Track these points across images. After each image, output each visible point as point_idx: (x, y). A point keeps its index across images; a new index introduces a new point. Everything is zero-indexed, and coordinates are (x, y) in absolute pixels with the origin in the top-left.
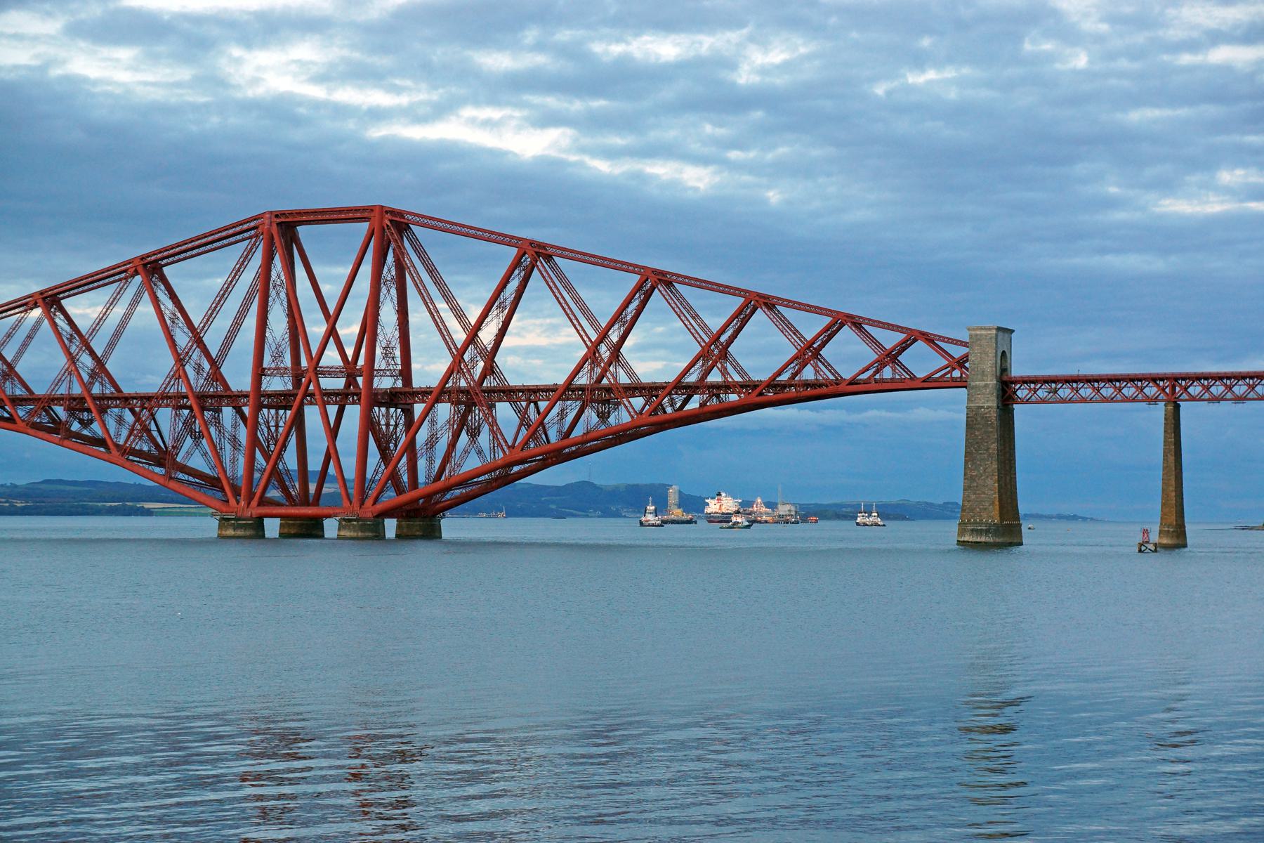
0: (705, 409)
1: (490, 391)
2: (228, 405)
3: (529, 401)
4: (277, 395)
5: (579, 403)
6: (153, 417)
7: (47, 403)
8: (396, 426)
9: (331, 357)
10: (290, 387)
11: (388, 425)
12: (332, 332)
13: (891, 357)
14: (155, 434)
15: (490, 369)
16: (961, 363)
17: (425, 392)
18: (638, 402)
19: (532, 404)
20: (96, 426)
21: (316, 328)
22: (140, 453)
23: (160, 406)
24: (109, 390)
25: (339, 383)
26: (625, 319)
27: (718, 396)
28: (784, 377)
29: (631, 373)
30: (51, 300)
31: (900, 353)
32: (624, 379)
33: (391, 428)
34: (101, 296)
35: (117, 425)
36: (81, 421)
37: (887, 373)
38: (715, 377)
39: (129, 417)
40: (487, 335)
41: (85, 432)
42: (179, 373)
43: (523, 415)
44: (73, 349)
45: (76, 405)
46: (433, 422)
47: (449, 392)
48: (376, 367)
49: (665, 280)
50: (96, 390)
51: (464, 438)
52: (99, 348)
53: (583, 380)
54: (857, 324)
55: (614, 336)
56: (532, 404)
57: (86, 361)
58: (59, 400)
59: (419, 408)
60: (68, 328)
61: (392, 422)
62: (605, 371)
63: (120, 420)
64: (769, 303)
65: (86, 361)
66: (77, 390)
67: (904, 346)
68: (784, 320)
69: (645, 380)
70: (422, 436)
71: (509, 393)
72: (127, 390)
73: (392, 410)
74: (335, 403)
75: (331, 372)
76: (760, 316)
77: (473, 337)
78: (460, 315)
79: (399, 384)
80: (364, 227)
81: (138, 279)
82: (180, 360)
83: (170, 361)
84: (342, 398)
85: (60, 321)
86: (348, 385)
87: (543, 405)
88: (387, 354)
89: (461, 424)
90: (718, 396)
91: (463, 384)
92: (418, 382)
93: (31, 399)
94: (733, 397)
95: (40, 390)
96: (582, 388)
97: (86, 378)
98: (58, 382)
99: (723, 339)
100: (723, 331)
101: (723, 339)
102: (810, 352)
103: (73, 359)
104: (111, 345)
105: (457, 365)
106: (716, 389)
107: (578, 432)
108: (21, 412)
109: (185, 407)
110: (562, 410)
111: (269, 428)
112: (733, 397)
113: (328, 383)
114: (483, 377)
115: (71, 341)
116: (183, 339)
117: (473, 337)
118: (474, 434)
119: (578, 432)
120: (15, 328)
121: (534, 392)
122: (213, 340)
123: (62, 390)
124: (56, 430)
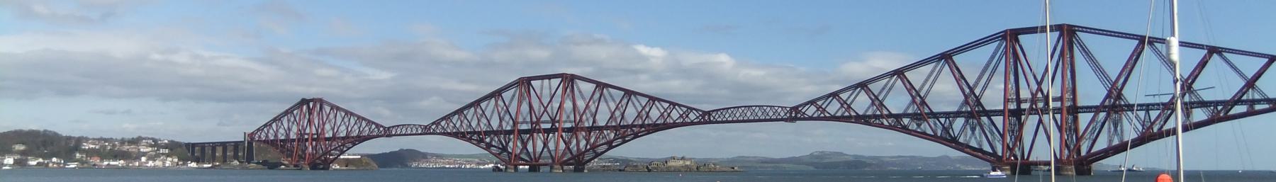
4: (1010, 111)
6: (951, 124)
7: (898, 117)
9: (1040, 95)
10: (1016, 107)
15: (1119, 96)
17: (1088, 109)
24: (927, 111)
30: (899, 73)
34: (927, 69)
38: (1250, 95)
41: (919, 130)
42: (966, 102)
45: (914, 117)
47: (1106, 107)
49: (1213, 50)
53: (1107, 103)
58: (905, 115)
59: (1023, 117)
69: (1207, 96)
75: (1041, 101)
83: (963, 98)
86: (1044, 106)
92: (1080, 103)
93: (890, 115)
95: (894, 112)
98: (908, 108)
103: (913, 98)
104: (928, 92)
105: (1108, 96)
106: (1253, 102)
120: (886, 85)
121: (1147, 107)
123: (910, 111)
124: (905, 130)
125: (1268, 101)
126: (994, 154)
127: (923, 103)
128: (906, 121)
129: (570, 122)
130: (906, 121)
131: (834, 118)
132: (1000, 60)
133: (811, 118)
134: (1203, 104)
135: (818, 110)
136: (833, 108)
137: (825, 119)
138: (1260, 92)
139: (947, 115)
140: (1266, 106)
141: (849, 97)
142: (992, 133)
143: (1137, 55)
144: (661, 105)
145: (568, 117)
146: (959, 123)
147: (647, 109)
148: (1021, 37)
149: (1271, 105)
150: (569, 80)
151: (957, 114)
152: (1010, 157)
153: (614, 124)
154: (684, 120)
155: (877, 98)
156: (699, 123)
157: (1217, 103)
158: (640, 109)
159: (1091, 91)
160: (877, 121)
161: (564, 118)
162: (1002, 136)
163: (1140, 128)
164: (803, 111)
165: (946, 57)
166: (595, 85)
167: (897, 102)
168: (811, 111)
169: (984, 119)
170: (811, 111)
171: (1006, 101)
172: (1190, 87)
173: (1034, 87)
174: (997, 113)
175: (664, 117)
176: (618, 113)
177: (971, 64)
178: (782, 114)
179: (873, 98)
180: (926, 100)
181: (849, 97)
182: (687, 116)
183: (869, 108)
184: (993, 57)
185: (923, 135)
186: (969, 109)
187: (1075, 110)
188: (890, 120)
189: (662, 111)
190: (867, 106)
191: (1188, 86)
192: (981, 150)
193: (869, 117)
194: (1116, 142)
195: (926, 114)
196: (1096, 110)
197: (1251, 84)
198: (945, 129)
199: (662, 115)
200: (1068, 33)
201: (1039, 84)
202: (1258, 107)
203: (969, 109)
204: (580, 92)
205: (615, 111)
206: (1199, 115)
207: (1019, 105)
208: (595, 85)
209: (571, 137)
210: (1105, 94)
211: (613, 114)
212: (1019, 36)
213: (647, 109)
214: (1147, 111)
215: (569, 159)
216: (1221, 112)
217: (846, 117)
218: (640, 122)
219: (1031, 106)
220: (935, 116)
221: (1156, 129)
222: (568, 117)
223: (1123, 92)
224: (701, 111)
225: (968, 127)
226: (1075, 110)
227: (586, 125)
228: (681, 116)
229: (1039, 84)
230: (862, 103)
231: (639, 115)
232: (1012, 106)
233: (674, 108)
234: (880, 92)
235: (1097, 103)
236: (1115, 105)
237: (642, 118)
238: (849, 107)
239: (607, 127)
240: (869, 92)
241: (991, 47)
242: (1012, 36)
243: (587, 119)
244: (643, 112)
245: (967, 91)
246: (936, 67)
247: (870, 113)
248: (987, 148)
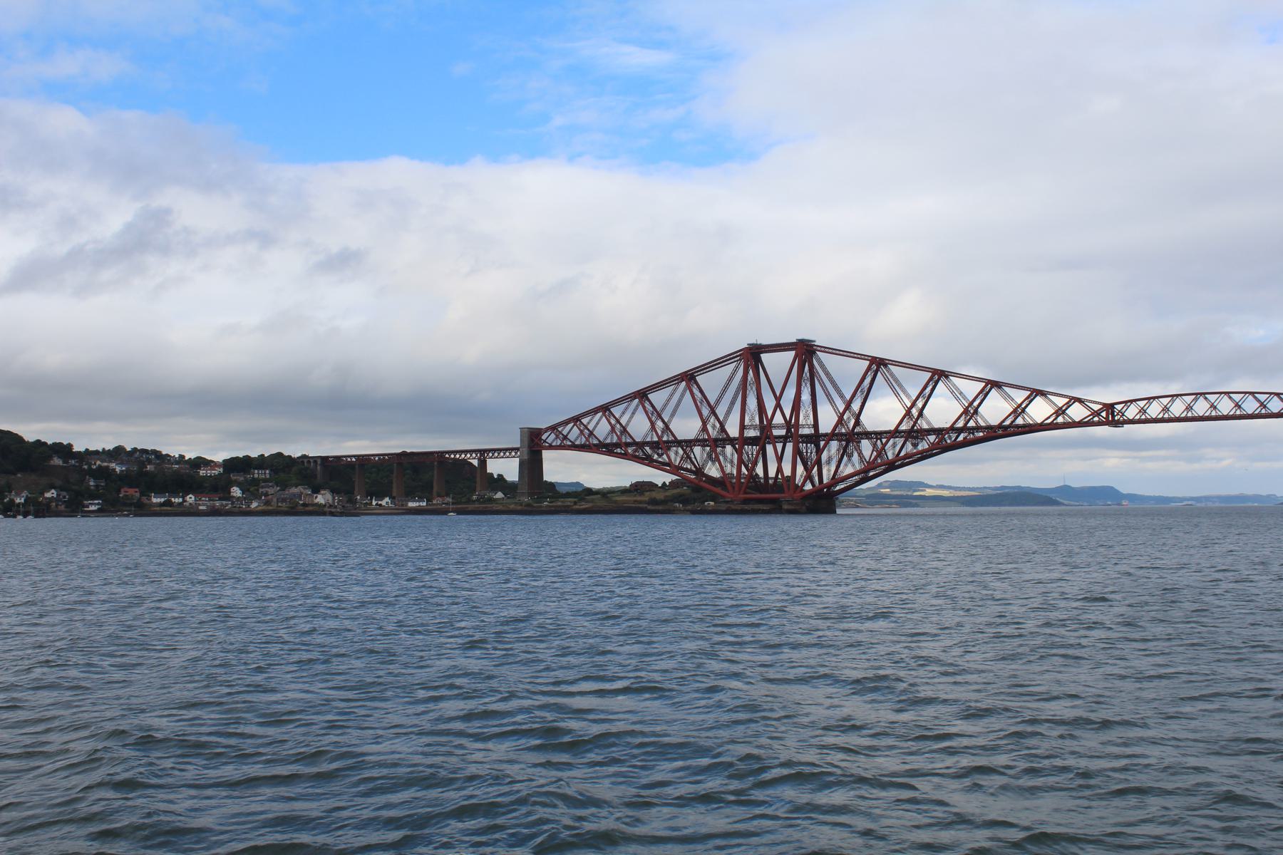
0: (966, 440)
1: (858, 434)
2: (728, 444)
3: (877, 439)
5: (903, 439)
7: (641, 445)
8: (811, 453)
9: (778, 419)
10: (758, 434)
11: (807, 452)
12: (778, 406)
14: (694, 459)
15: (857, 423)
16: (1097, 413)
17: (826, 435)
18: (932, 438)
19: (879, 441)
20: (665, 456)
21: (770, 404)
22: (686, 470)
23: (695, 446)
24: (671, 438)
25: (783, 432)
26: (926, 394)
27: (973, 434)
28: (1007, 423)
29: (928, 423)
31: (1066, 409)
32: (925, 426)
33: (809, 454)
35: (675, 455)
36: (658, 454)
37: (1060, 420)
38: (971, 424)
39: (681, 451)
40: (856, 406)
41: (660, 460)
42: (704, 429)
43: (874, 445)
44: (653, 419)
45: (654, 446)
46: (829, 451)
47: (837, 435)
48: (800, 423)
50: (665, 438)
51: (845, 458)
53: (904, 427)
55: (920, 404)
56: (879, 441)
57: (659, 424)
58: (647, 443)
59: (822, 443)
60: (651, 409)
61: (809, 451)
62: (915, 423)
63: (677, 453)
64: (996, 385)
65: (659, 424)
66: (656, 439)
67: (1068, 405)
68: (1006, 393)
69: (936, 426)
70: (824, 456)
71: (867, 435)
73: (809, 445)
74: (781, 442)
75: (778, 427)
77: (848, 406)
78: (842, 396)
81: (684, 383)
82: (704, 423)
84: (784, 439)
85: (647, 405)
86: (787, 432)
87: (884, 440)
88: (806, 416)
89: (844, 452)
90: (973, 434)
91: (843, 431)
93: (634, 443)
94: (981, 434)
96: (903, 431)
97: (660, 433)
98: (646, 435)
99: (976, 404)
100: (974, 400)
101: (976, 404)
102: (1019, 411)
103: (653, 424)
105: (840, 421)
107: (902, 454)
108: (630, 450)
109: (707, 446)
110: (894, 443)
111: (748, 456)
112: (981, 434)
113: (776, 432)
114: (854, 427)
115: (652, 414)
116: (706, 412)
117: (848, 406)
118: (850, 456)
119: (902, 454)
121: (879, 435)
122: (721, 412)
123: (648, 439)
125: (989, 428)
131: (574, 447)
135: (557, 437)
139: (688, 444)
141: (588, 423)
148: (764, 357)
155: (618, 421)
159: (827, 421)
160: (619, 450)
179: (613, 421)
185: (661, 466)
195: (667, 442)
197: (970, 411)
198: (687, 457)
220: (679, 443)
230: (602, 428)
238: (591, 433)
242: (752, 355)
246: (675, 390)
247: (608, 441)
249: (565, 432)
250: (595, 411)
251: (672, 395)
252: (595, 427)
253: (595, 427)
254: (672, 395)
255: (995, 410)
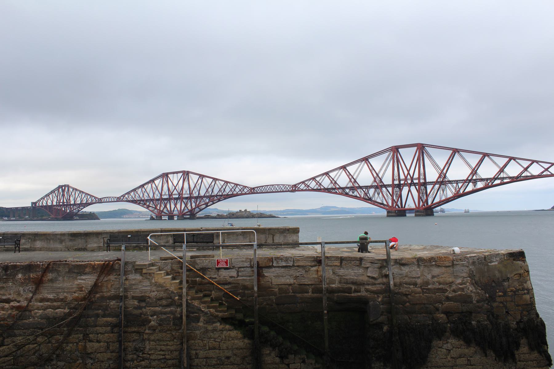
4: (396, 185)
6: (368, 191)
9: (409, 177)
10: (398, 183)
13: (547, 170)
15: (445, 177)
17: (431, 183)
24: (357, 185)
30: (344, 167)
38: (502, 175)
41: (353, 195)
42: (375, 181)
44: (350, 178)
47: (439, 182)
52: (355, 178)
54: (537, 162)
64: (514, 159)
65: (353, 180)
69: (483, 177)
71: (450, 182)
72: (361, 185)
76: (512, 160)
79: (424, 181)
80: (416, 148)
81: (364, 161)
82: (375, 179)
83: (373, 179)
86: (411, 182)
93: (340, 188)
103: (350, 179)
104: (357, 176)
105: (439, 177)
106: (503, 178)
121: (457, 182)
123: (349, 186)
124: (347, 195)
125: (510, 178)
126: (388, 205)
127: (355, 181)
128: (347, 191)
129: (187, 194)
130: (347, 191)
132: (390, 160)
133: (302, 190)
134: (482, 180)
135: (305, 186)
136: (313, 185)
137: (309, 190)
138: (506, 174)
139: (367, 187)
140: (509, 180)
141: (320, 180)
142: (387, 195)
143: (452, 157)
144: (231, 185)
145: (186, 192)
146: (372, 191)
147: (224, 187)
149: (511, 180)
150: (186, 174)
151: (371, 187)
152: (395, 206)
153: (208, 195)
154: (242, 192)
155: (333, 179)
156: (249, 194)
157: (487, 179)
158: (220, 187)
159: (432, 175)
160: (334, 191)
161: (184, 192)
162: (392, 196)
163: (454, 191)
164: (299, 186)
165: (366, 159)
166: (199, 176)
167: (326, 183)
168: (302, 187)
169: (384, 189)
170: (302, 187)
171: (393, 180)
172: (476, 172)
173: (406, 173)
174: (389, 186)
175: (232, 191)
176: (210, 190)
177: (376, 163)
178: (289, 188)
179: (331, 179)
180: (337, 182)
181: (320, 180)
182: (243, 190)
183: (330, 184)
184: (387, 159)
185: (356, 197)
186: (376, 184)
187: (425, 184)
188: (340, 190)
189: (231, 188)
190: (314, 185)
191: (474, 172)
192: (382, 204)
193: (330, 189)
194: (443, 198)
195: (357, 187)
196: (434, 183)
197: (502, 170)
198: (366, 194)
199: (231, 190)
200: (421, 148)
201: (408, 171)
202: (505, 181)
203: (376, 184)
204: (192, 179)
205: (209, 187)
206: (480, 185)
207: (400, 182)
208: (199, 176)
209: (167, 203)
210: (438, 176)
211: (207, 190)
212: (399, 149)
213: (224, 187)
214: (457, 183)
215: (187, 212)
216: (489, 184)
217: (308, 190)
218: (221, 194)
219: (405, 182)
220: (361, 187)
221: (461, 191)
222: (186, 192)
223: (446, 175)
224: (249, 187)
225: (376, 193)
226: (425, 184)
227: (195, 195)
228: (240, 190)
229: (408, 171)
231: (220, 190)
232: (396, 182)
233: (237, 186)
234: (335, 177)
235: (435, 180)
236: (442, 182)
237: (221, 191)
238: (320, 184)
239: (204, 196)
240: (329, 177)
241: (386, 154)
242: (395, 150)
243: (195, 193)
244: (222, 189)
245: (375, 175)
246: (360, 164)
247: (330, 187)
248: (385, 203)
249: (308, 184)
250: (323, 174)
251: (359, 167)
252: (338, 179)
253: (338, 179)
254: (359, 167)
255: (513, 170)
